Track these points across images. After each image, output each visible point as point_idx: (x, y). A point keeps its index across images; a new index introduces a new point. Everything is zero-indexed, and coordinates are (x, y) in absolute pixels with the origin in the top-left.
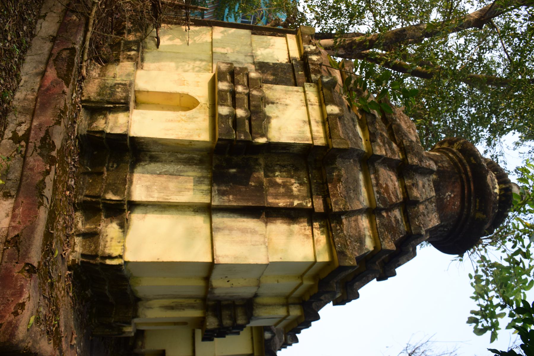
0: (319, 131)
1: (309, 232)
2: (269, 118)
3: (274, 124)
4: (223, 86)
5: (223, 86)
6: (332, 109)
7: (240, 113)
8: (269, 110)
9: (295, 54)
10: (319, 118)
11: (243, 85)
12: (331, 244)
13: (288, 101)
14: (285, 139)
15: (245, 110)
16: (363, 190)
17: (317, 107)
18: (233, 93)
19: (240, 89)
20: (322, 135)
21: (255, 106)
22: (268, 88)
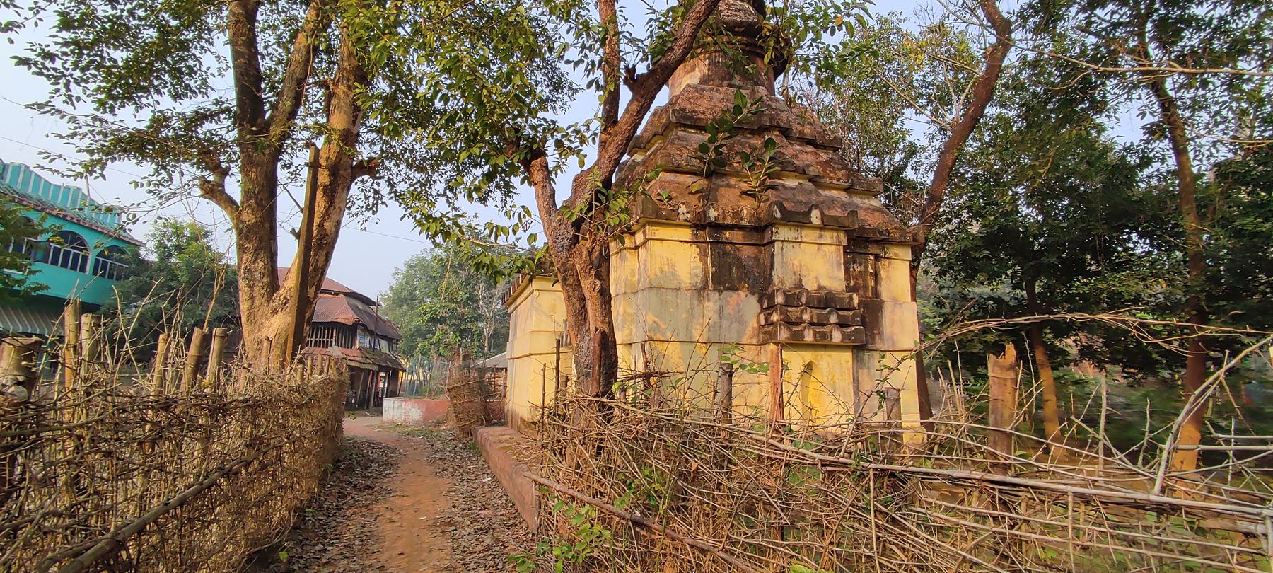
0: (829, 237)
1: (886, 262)
2: (820, 288)
3: (823, 283)
4: (809, 336)
5: (809, 336)
6: (815, 217)
7: (833, 319)
8: (810, 285)
9: (686, 234)
10: (817, 233)
11: (802, 312)
12: (901, 244)
13: (796, 263)
14: (842, 275)
15: (830, 313)
16: (834, 193)
17: (805, 232)
18: (812, 324)
19: (806, 317)
20: (835, 234)
21: (820, 302)
22: (782, 281)
